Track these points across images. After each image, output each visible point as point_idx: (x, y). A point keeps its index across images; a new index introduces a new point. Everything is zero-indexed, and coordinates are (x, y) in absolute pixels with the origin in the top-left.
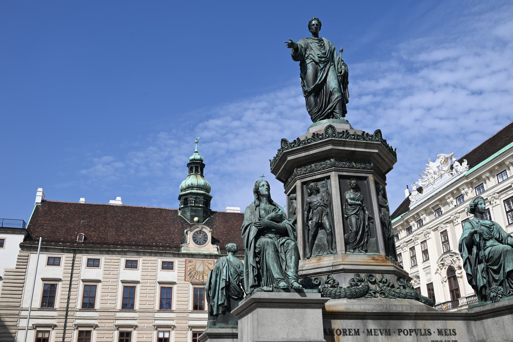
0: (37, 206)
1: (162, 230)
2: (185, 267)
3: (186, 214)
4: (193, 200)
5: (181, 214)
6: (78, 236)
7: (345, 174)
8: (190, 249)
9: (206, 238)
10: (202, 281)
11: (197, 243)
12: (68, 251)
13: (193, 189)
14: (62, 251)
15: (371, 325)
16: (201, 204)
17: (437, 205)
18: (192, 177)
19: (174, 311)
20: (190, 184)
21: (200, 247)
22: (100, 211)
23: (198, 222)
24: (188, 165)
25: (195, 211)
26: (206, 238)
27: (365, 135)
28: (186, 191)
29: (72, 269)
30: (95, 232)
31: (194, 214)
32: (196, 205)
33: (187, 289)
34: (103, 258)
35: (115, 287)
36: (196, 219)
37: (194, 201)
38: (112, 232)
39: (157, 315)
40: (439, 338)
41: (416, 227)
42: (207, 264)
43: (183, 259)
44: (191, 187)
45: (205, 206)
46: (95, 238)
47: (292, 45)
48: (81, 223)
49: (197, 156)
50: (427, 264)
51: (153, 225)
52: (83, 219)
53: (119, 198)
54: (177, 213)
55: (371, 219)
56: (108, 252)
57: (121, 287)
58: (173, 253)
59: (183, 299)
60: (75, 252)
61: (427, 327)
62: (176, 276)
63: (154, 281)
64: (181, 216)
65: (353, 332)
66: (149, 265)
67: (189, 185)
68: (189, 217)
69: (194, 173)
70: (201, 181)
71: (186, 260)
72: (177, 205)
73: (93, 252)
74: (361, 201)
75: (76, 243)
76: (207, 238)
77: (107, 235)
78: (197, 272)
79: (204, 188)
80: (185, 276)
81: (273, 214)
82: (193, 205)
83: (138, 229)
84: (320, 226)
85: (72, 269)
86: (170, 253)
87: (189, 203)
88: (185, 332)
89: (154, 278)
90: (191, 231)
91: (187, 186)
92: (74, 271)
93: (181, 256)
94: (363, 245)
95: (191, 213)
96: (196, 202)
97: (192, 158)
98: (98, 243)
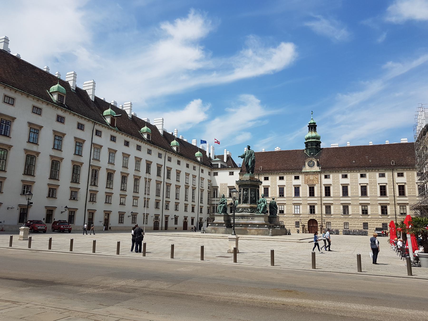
7: (244, 188)
11: (310, 167)
18: (309, 132)
23: (313, 155)
24: (308, 126)
32: (312, 147)
33: (306, 187)
35: (276, 188)
36: (312, 153)
39: (294, 199)
44: (309, 138)
45: (316, 147)
46: (267, 168)
47: (239, 157)
49: (312, 121)
51: (292, 159)
53: (278, 147)
54: (304, 152)
55: (248, 197)
63: (291, 185)
67: (308, 138)
68: (309, 153)
70: (313, 134)
72: (304, 147)
74: (247, 194)
76: (314, 164)
79: (316, 138)
81: (223, 200)
82: (310, 147)
83: (285, 162)
88: (306, 206)
89: (291, 183)
90: (307, 161)
93: (303, 173)
97: (309, 122)
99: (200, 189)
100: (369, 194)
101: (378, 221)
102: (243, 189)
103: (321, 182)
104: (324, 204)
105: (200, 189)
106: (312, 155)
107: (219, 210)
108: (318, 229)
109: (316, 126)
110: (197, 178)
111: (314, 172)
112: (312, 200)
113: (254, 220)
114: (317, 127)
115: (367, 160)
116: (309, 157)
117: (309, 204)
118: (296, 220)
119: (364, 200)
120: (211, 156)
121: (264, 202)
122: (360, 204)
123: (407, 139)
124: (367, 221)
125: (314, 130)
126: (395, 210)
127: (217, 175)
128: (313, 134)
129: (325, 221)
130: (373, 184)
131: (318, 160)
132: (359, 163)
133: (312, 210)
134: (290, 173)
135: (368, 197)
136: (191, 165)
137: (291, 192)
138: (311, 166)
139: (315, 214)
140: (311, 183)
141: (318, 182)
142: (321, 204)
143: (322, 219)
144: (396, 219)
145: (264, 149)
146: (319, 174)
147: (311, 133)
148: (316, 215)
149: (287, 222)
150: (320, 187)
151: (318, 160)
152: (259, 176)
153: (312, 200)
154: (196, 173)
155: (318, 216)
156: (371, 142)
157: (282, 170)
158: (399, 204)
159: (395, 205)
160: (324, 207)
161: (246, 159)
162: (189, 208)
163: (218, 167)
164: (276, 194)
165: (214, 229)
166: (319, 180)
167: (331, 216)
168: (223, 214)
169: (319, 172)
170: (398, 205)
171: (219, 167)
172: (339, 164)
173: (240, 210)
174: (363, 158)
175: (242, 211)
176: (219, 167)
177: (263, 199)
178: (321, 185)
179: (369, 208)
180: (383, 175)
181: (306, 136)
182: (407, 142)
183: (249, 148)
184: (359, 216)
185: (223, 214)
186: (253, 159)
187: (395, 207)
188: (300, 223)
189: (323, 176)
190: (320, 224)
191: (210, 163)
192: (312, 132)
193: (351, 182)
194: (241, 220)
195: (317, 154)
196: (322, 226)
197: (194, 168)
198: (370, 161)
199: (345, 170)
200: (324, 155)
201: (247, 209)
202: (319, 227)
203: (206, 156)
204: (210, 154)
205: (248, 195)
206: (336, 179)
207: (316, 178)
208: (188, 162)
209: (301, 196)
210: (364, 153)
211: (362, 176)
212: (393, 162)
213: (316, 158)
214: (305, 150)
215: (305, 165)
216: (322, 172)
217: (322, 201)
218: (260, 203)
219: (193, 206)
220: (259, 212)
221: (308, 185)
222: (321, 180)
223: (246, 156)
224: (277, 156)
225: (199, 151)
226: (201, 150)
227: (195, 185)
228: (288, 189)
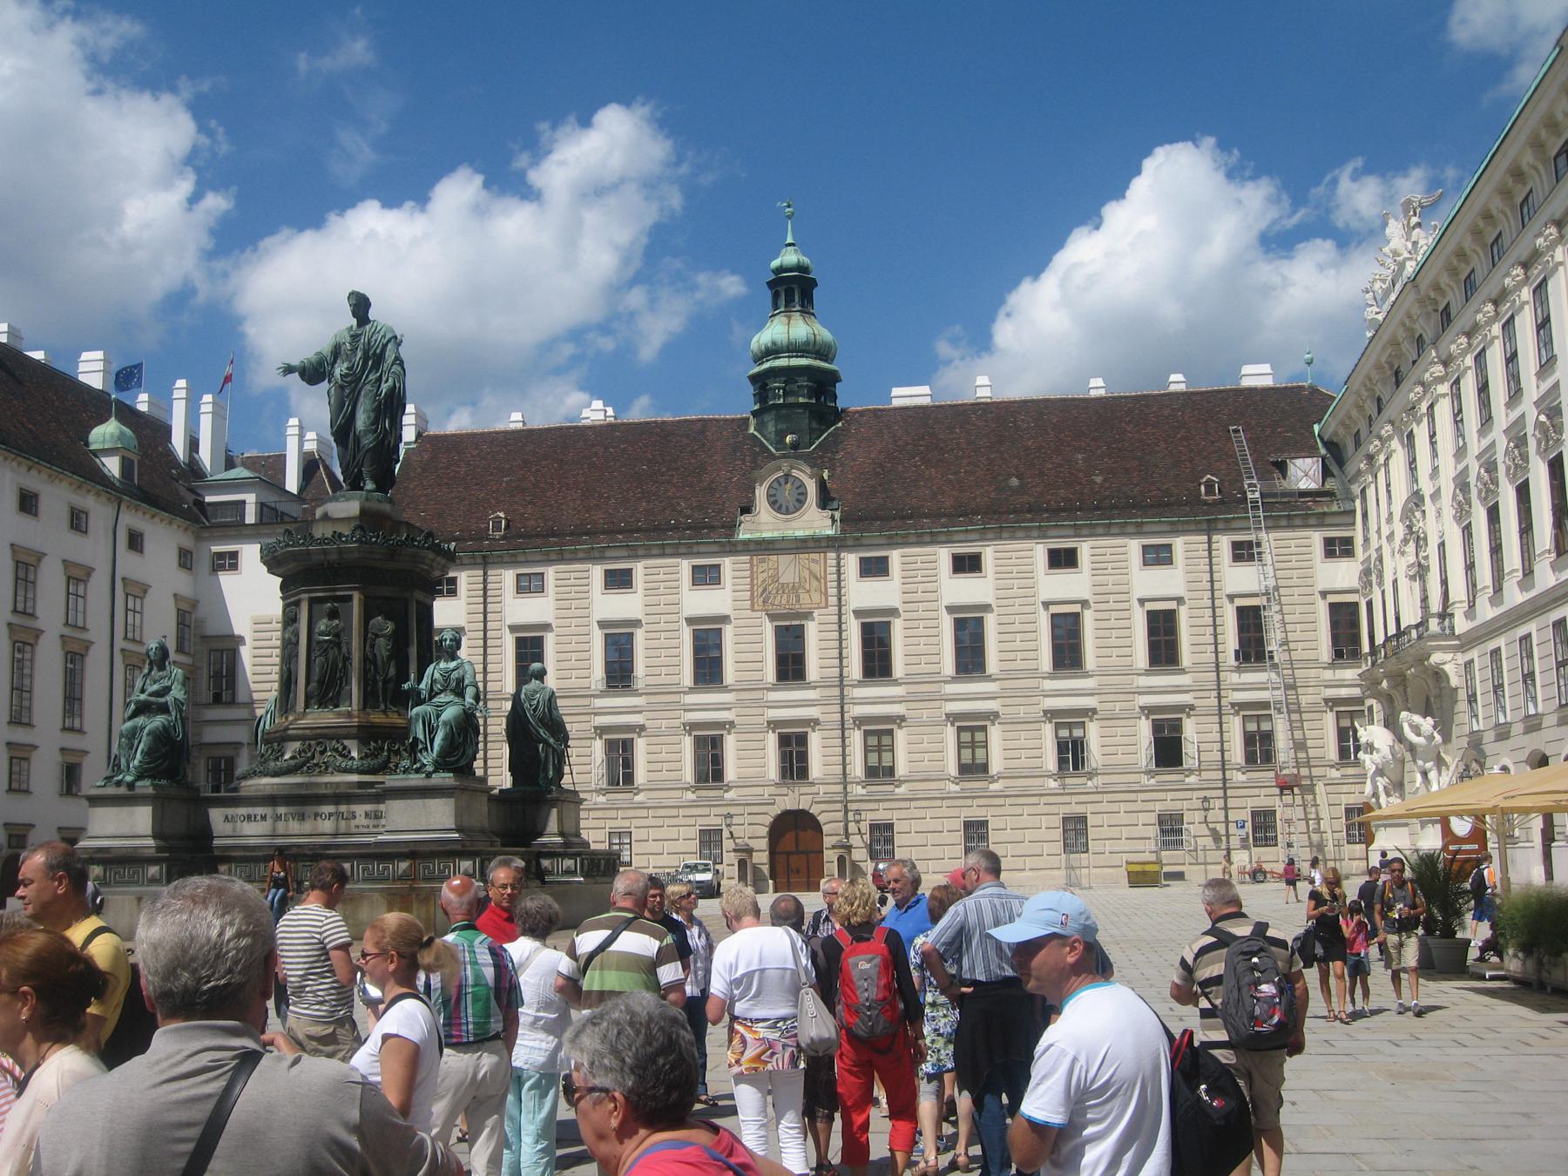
0: (407, 450)
2: (752, 577)
4: (779, 389)
5: (755, 429)
8: (763, 528)
10: (798, 606)
11: (779, 510)
13: (780, 357)
15: (282, 810)
16: (803, 396)
18: (777, 319)
21: (787, 521)
23: (795, 446)
24: (771, 284)
27: (336, 536)
28: (763, 363)
29: (485, 603)
31: (784, 426)
32: (791, 400)
33: (758, 630)
37: (784, 389)
39: (691, 699)
40: (364, 822)
41: (1376, 414)
42: (806, 562)
44: (772, 351)
47: (289, 370)
48: (504, 485)
49: (790, 257)
51: (676, 469)
55: (347, 659)
59: (750, 657)
60: (485, 564)
62: (729, 601)
64: (755, 433)
65: (259, 818)
66: (662, 577)
68: (773, 436)
69: (783, 309)
70: (798, 329)
74: (337, 635)
75: (487, 540)
76: (805, 494)
77: (562, 510)
78: (783, 587)
79: (811, 348)
81: (155, 687)
82: (781, 401)
84: (289, 671)
85: (485, 603)
87: (770, 395)
88: (759, 736)
92: (490, 607)
94: (331, 699)
95: (776, 426)
97: (775, 263)
99: (123, 650)
100: (1090, 658)
101: (1139, 806)
102: (312, 601)
103: (840, 599)
104: (860, 721)
105: (123, 650)
107: (123, 761)
108: (826, 865)
109: (813, 283)
110: (100, 583)
112: (792, 703)
113: (383, 821)
114: (815, 292)
115: (1081, 475)
116: (774, 458)
117: (774, 724)
118: (701, 821)
119: (1068, 692)
120: (205, 455)
121: (460, 692)
122: (1051, 714)
123: (1268, 365)
125: (802, 306)
126: (1222, 742)
127: (234, 567)
128: (798, 329)
129: (863, 817)
130: (1111, 605)
131: (825, 476)
132: (1039, 490)
134: (668, 551)
135: (1087, 675)
136: (57, 495)
137: (674, 661)
139: (810, 780)
140: (782, 602)
142: (843, 725)
143: (846, 806)
144: (1225, 789)
145: (516, 416)
147: (784, 319)
148: (813, 784)
149: (653, 833)
150: (836, 627)
151: (826, 477)
153: (792, 703)
154: (92, 549)
155: (822, 789)
156: (1099, 382)
157: (620, 533)
158: (1239, 707)
159: (1220, 715)
160: (856, 738)
161: (342, 388)
162: (45, 772)
163: (243, 515)
164: (585, 673)
166: (829, 584)
167: (897, 790)
168: (150, 790)
170: (1237, 713)
171: (250, 518)
173: (287, 756)
174: (1060, 465)
175: (303, 764)
176: (250, 518)
177: (452, 665)
178: (840, 615)
179: (1094, 734)
180: (1158, 557)
181: (755, 339)
182: (1268, 382)
183: (360, 305)
184: (1038, 781)
185: (145, 787)
186: (385, 387)
187: (1221, 724)
188: (726, 834)
189: (851, 561)
190: (838, 838)
191: (194, 497)
192: (789, 318)
193: (1002, 593)
194: (294, 826)
195: (817, 443)
196: (849, 848)
197: (78, 521)
198: (1099, 479)
199: (967, 530)
200: (859, 447)
201: (336, 750)
202: (830, 856)
203: (170, 454)
204: (193, 444)
205: (349, 644)
206: (919, 579)
207: (818, 580)
208: (36, 481)
210: (1066, 436)
212: (1210, 487)
213: (815, 462)
214: (753, 422)
217: (846, 707)
218: (431, 698)
219: (72, 759)
220: (418, 765)
221: (772, 617)
222: (839, 588)
223: (340, 369)
224: (596, 453)
225: (113, 419)
226: (128, 415)
227: (84, 629)
228: (655, 643)
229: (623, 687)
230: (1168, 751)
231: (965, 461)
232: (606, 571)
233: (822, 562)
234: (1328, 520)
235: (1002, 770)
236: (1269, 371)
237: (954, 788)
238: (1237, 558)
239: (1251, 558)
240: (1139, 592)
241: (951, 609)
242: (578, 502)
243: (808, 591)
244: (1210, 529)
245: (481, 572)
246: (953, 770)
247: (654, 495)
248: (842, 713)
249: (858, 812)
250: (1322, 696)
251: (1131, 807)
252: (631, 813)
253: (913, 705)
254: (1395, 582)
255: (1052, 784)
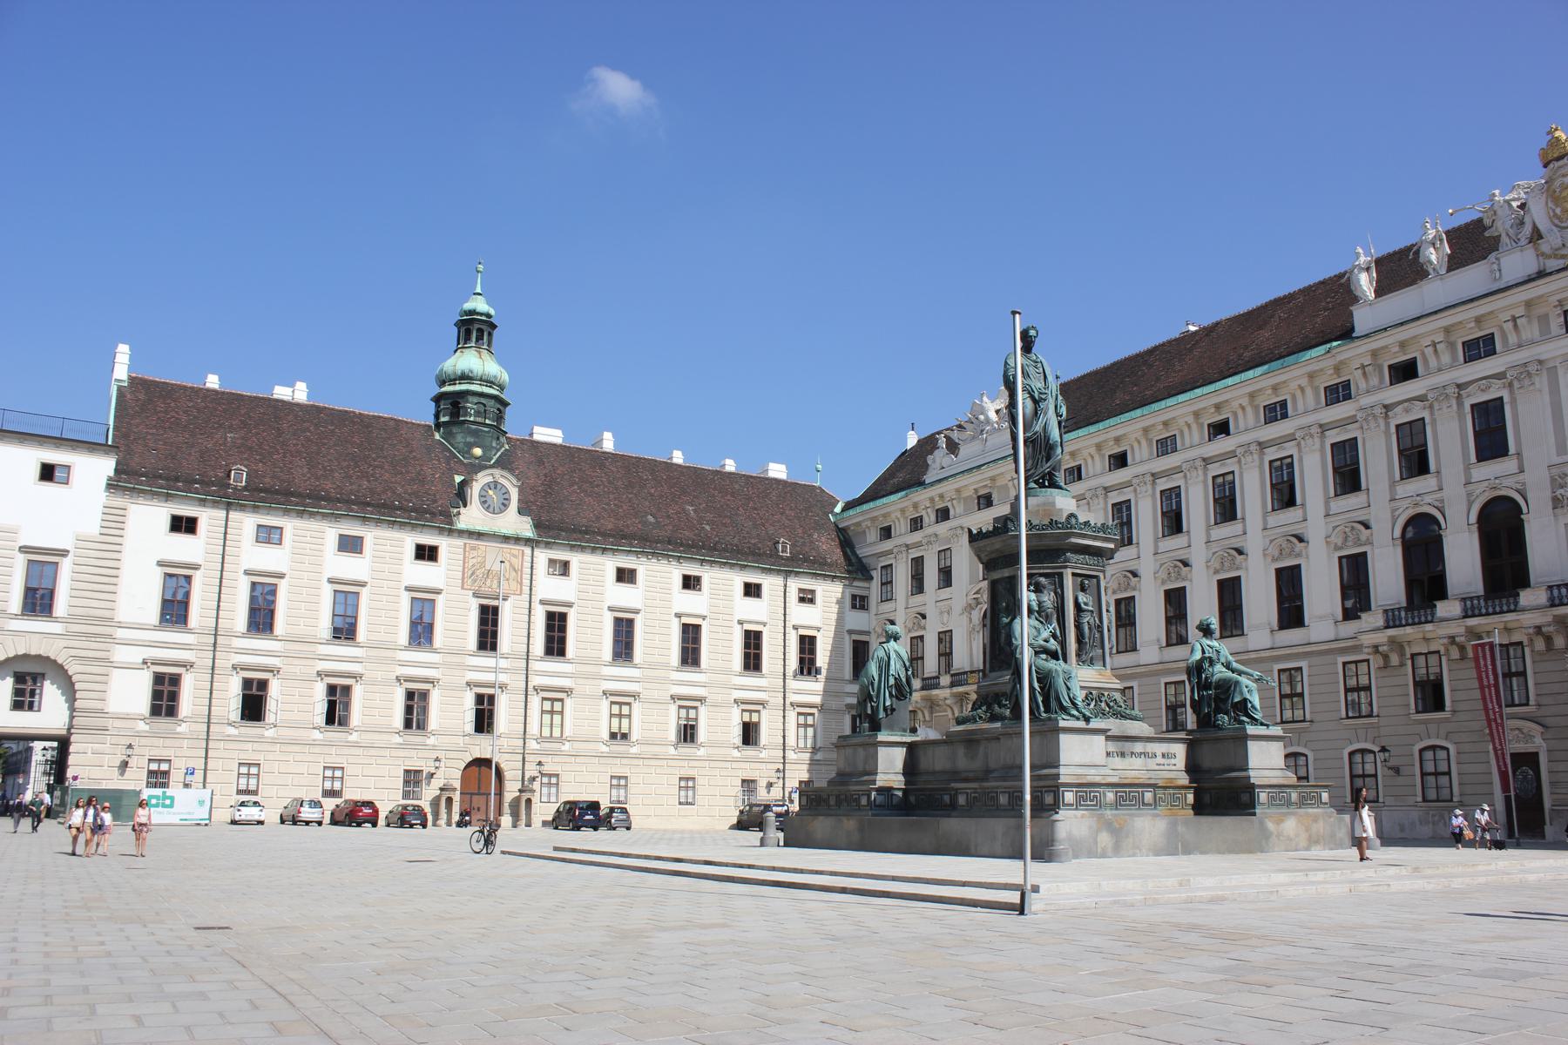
0: (120, 389)
1: (407, 472)
2: (464, 558)
3: (454, 437)
4: (471, 409)
6: (233, 472)
9: (507, 499)
11: (487, 509)
12: (215, 504)
14: (203, 503)
16: (489, 419)
17: (986, 486)
19: (438, 651)
20: (467, 371)
22: (264, 414)
25: (475, 433)
26: (507, 499)
28: (455, 384)
30: (264, 463)
31: (472, 440)
34: (291, 526)
36: (478, 451)
38: (301, 467)
41: (933, 517)
43: (459, 542)
45: (495, 424)
48: (229, 439)
49: (480, 305)
50: (945, 593)
51: (385, 457)
52: (231, 429)
54: (433, 435)
56: (300, 514)
57: (327, 592)
58: (439, 527)
61: (1154, 751)
71: (465, 544)
73: (269, 510)
80: (463, 579)
82: (472, 419)
86: (430, 526)
87: (461, 413)
91: (459, 373)
96: (478, 413)
97: (468, 306)
98: (277, 492)
106: (477, 458)
109: (494, 326)
111: (506, 539)
113: (1173, 761)
124: (690, 773)
133: (484, 720)
138: (491, 509)
140: (490, 586)
141: (521, 587)
142: (527, 691)
144: (784, 763)
146: (528, 551)
152: (233, 515)
160: (535, 701)
165: (1109, 826)
169: (527, 541)
172: (598, 518)
187: (784, 717)
198: (708, 528)
199: (630, 551)
207: (514, 569)
209: (360, 641)
211: (690, 583)
215: (461, 496)
216: (538, 542)
221: (476, 595)
229: (346, 638)
230: (749, 734)
231: (611, 496)
232: (341, 536)
233: (520, 558)
234: (856, 583)
235: (640, 738)
236: (785, 470)
237: (605, 749)
238: (802, 600)
239: (812, 601)
240: (738, 617)
241: (611, 609)
242: (306, 470)
243: (507, 580)
244: (787, 574)
245: (225, 512)
246: (606, 736)
247: (372, 476)
248: (527, 682)
249: (540, 763)
250: (845, 703)
251: (724, 773)
252: (346, 751)
253: (581, 681)
254: (945, 638)
255: (672, 750)
